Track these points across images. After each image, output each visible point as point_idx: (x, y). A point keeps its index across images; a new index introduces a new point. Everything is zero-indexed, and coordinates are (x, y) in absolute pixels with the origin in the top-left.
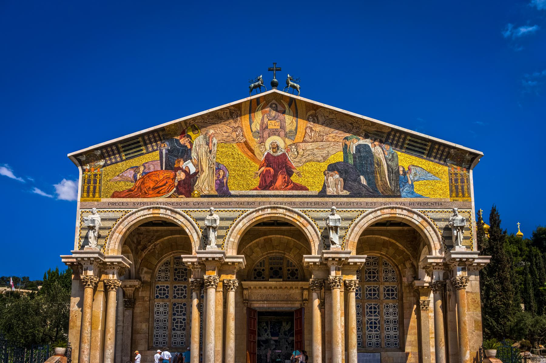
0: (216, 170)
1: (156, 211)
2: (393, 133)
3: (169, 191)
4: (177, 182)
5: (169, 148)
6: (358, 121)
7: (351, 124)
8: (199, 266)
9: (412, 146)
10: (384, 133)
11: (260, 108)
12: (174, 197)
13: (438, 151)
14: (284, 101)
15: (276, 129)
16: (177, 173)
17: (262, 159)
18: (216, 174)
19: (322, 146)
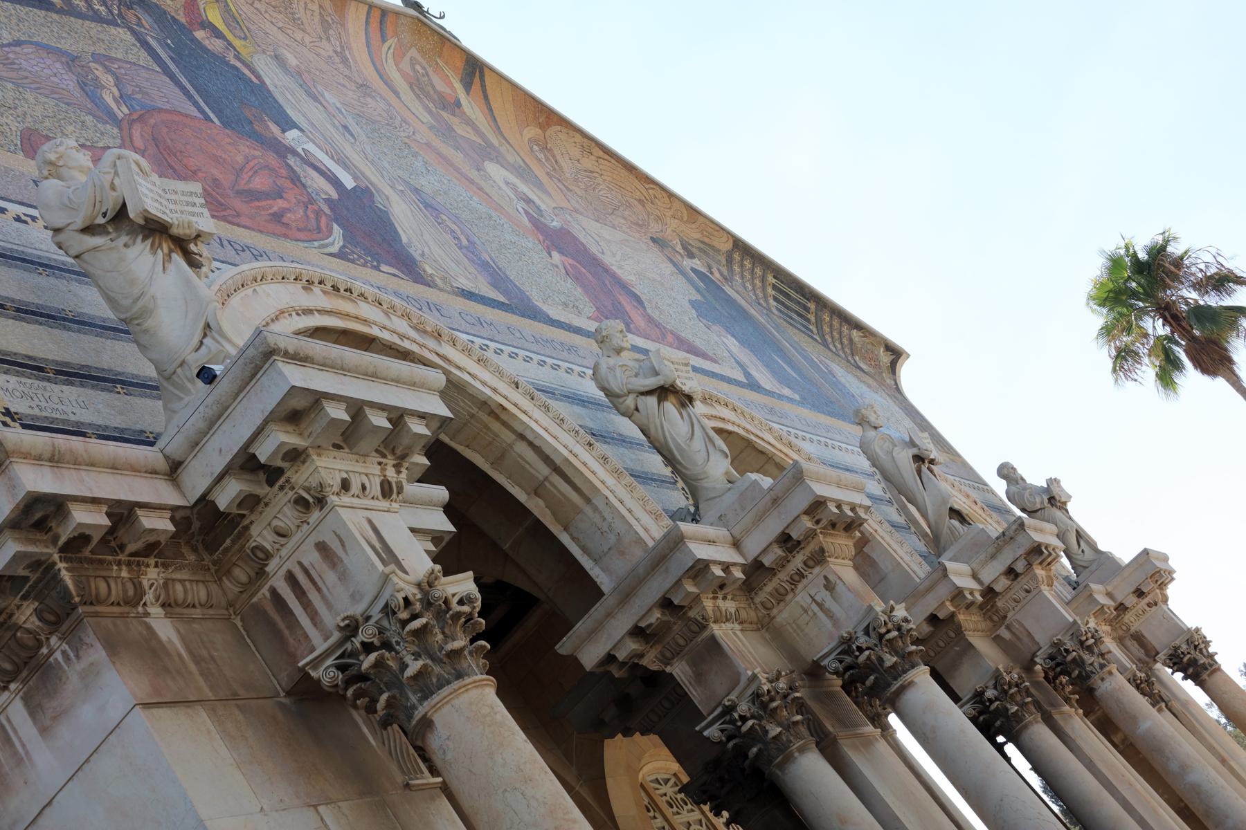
0: (425, 207)
1: (346, 306)
2: (737, 257)
3: (319, 230)
4: (321, 201)
5: (169, 42)
6: (655, 197)
7: (640, 201)
8: (729, 606)
9: (782, 304)
10: (718, 251)
11: (390, 55)
12: (364, 265)
13: (831, 333)
14: (446, 63)
15: (480, 145)
16: (289, 161)
17: (526, 220)
18: (439, 224)
19: (627, 240)
